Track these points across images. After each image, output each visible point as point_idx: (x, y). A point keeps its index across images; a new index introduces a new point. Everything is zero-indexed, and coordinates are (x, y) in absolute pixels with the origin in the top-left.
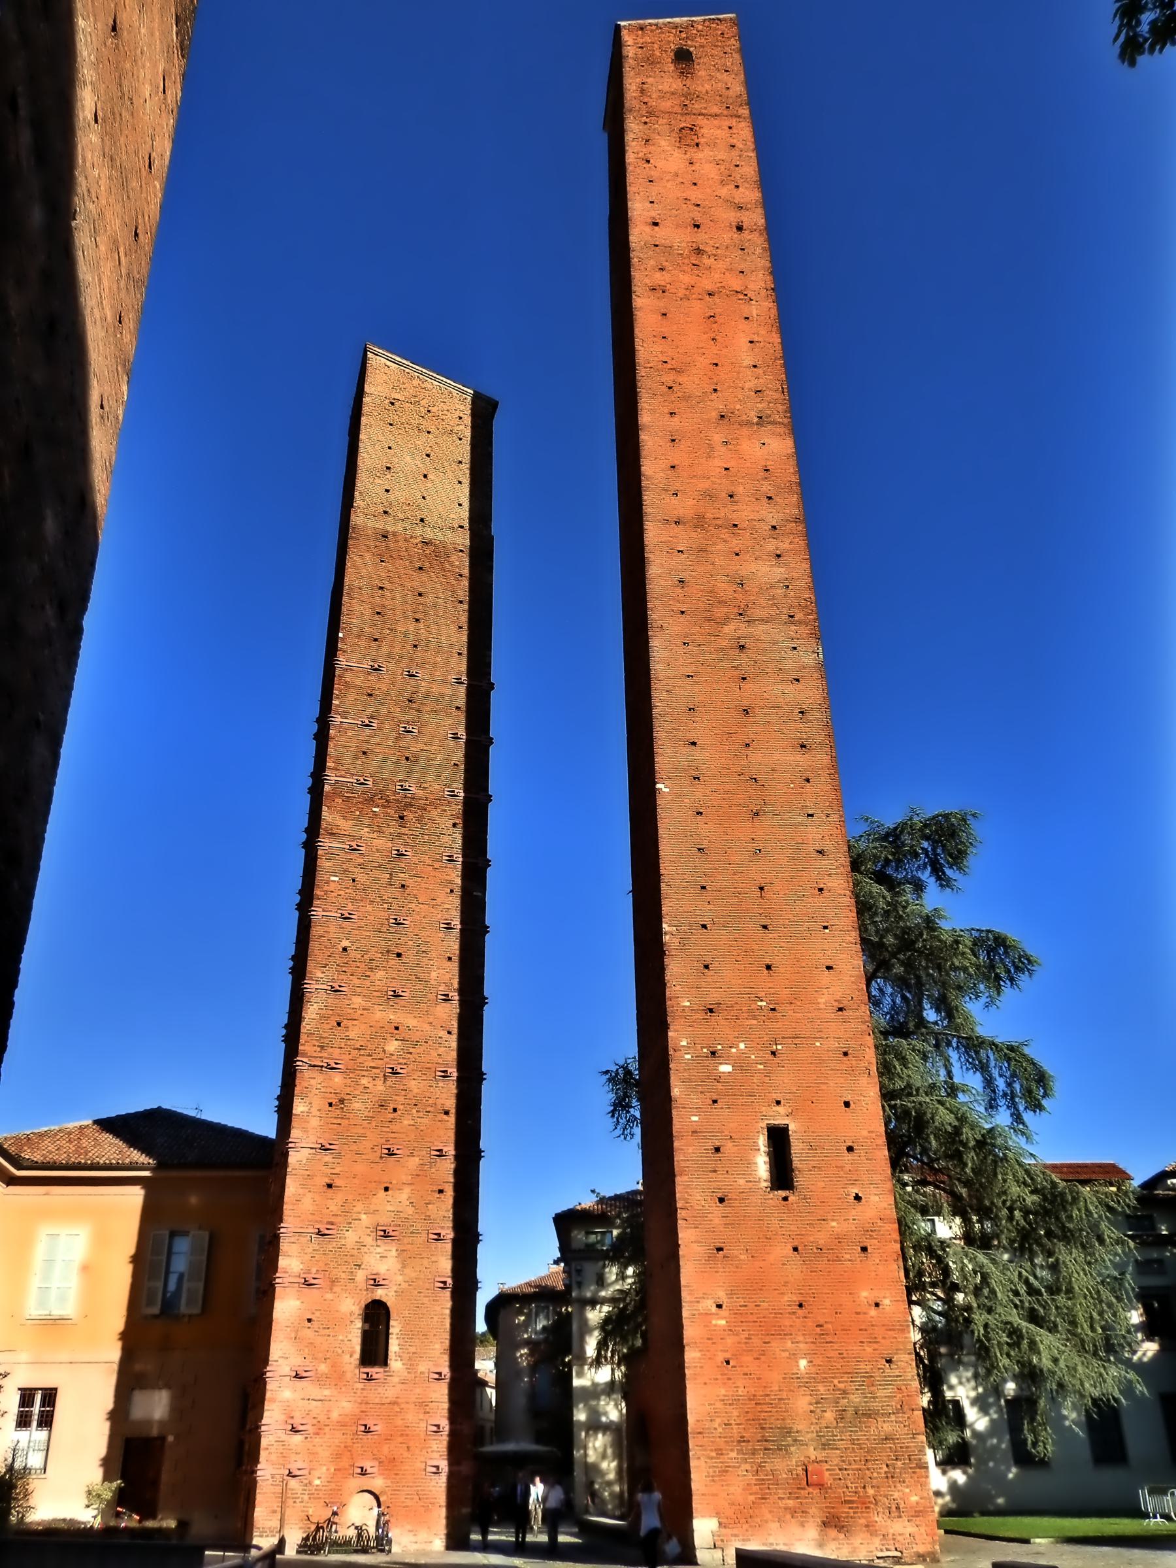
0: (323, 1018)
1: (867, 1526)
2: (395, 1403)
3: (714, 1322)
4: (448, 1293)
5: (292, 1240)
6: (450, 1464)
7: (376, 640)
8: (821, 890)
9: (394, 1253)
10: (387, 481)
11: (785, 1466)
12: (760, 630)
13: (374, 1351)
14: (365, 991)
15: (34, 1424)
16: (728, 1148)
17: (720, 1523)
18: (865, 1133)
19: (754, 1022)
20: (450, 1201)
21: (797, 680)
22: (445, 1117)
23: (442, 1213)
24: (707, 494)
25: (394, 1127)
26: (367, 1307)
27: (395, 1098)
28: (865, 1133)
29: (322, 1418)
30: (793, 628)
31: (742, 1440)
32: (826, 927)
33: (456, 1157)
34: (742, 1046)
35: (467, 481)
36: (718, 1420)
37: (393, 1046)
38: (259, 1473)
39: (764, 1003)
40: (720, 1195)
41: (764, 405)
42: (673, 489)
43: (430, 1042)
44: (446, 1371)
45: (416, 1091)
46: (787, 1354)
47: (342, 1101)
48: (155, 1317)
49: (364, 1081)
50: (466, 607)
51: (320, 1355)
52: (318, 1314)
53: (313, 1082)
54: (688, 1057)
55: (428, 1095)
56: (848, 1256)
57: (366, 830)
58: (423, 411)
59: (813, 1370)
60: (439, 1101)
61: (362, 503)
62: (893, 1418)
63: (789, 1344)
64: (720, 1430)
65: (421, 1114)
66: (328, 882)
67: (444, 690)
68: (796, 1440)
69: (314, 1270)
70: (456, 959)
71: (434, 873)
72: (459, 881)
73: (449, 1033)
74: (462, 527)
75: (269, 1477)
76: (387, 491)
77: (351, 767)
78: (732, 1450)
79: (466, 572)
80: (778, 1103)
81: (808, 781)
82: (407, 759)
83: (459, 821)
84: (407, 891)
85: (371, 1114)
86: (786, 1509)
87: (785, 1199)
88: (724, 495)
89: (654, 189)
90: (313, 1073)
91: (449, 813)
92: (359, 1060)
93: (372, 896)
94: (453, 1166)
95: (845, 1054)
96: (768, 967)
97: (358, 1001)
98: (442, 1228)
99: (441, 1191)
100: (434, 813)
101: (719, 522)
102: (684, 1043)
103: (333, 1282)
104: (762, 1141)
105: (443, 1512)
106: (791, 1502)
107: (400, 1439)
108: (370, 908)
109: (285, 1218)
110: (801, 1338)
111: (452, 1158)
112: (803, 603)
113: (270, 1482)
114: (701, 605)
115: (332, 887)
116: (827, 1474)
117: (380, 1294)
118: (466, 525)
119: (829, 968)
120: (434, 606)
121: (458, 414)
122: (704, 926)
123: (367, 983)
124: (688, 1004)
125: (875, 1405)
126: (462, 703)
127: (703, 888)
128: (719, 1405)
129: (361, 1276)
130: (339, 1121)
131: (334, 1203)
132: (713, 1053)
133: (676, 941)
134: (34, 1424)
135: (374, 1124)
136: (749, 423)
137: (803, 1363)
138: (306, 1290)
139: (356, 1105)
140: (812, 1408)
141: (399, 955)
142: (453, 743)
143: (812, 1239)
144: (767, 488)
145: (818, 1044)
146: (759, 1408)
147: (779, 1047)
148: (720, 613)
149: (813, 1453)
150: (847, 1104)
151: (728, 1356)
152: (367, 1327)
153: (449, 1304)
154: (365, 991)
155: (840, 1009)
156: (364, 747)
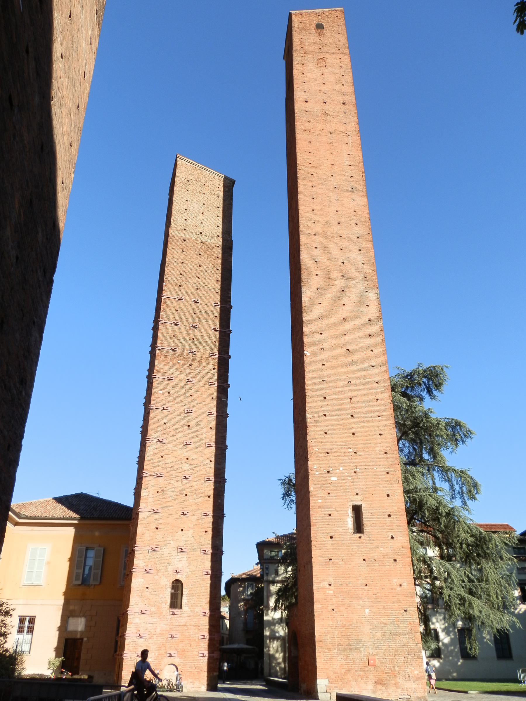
0: (155, 454)
1: (395, 684)
2: (185, 625)
3: (327, 592)
4: (209, 577)
5: (140, 552)
6: (209, 653)
7: (180, 286)
8: (377, 399)
9: (185, 559)
10: (185, 215)
11: (358, 657)
12: (351, 283)
13: (176, 602)
14: (174, 442)
15: (25, 631)
16: (334, 514)
17: (329, 682)
18: (396, 509)
19: (347, 458)
20: (210, 536)
21: (368, 306)
22: (209, 498)
23: (206, 542)
24: (328, 222)
25: (185, 503)
26: (173, 582)
27: (186, 490)
28: (396, 509)
29: (152, 631)
30: (366, 282)
31: (340, 645)
32: (379, 416)
33: (213, 516)
34: (341, 469)
35: (221, 216)
36: (329, 636)
37: (186, 467)
38: (124, 655)
39: (351, 450)
40: (331, 535)
41: (354, 183)
42: (313, 220)
43: (202, 465)
44: (208, 612)
45: (195, 487)
46: (360, 607)
47: (163, 491)
48: (79, 585)
49: (173, 482)
50: (220, 271)
51: (152, 603)
52: (151, 585)
53: (150, 482)
54: (317, 473)
55: (201, 488)
56: (388, 564)
57: (175, 370)
58: (202, 184)
59: (372, 614)
60: (206, 492)
61: (175, 226)
62: (407, 636)
63: (361, 602)
64: (330, 640)
65: (198, 497)
67: (210, 308)
68: (363, 645)
69: (150, 566)
70: (214, 428)
71: (204, 390)
72: (215, 394)
73: (211, 461)
74: (218, 236)
75: (129, 657)
76: (186, 220)
77: (168, 342)
78: (335, 649)
79: (220, 256)
80: (357, 494)
81: (372, 351)
82: (193, 339)
83: (216, 367)
84: (193, 398)
85: (175, 497)
86: (359, 676)
87: (360, 537)
88: (336, 223)
89: (306, 86)
90: (151, 478)
91: (211, 363)
92: (170, 473)
93: (177, 400)
94: (212, 520)
95: (388, 473)
96: (354, 434)
97: (170, 446)
98: (207, 548)
99: (206, 532)
100: (205, 363)
101: (333, 235)
102: (315, 467)
103: (158, 571)
104: (350, 512)
105: (206, 674)
106: (361, 672)
107: (187, 641)
108: (176, 405)
109: (137, 542)
110: (366, 600)
111: (211, 517)
112: (371, 271)
113: (129, 659)
114: (325, 271)
115: (159, 396)
116: (377, 661)
117: (179, 577)
118: (221, 235)
119: (381, 434)
120: (206, 271)
121: (217, 186)
122: (325, 415)
123: (175, 438)
124: (317, 450)
125: (399, 630)
126: (218, 315)
127: (325, 398)
128: (329, 629)
129: (170, 569)
130: (161, 500)
131: (159, 535)
132: (328, 472)
133: (312, 421)
134: (25, 631)
135: (177, 501)
136: (347, 191)
137: (367, 611)
138: (146, 574)
139: (169, 493)
140: (371, 631)
141: (189, 426)
142: (214, 332)
143: (371, 555)
144: (355, 220)
145: (375, 468)
146: (347, 630)
147: (358, 470)
148: (333, 275)
149: (371, 651)
150: (388, 496)
151: (333, 607)
152: (173, 591)
153: (209, 582)
154: (174, 442)
155: (386, 453)
156: (174, 334)
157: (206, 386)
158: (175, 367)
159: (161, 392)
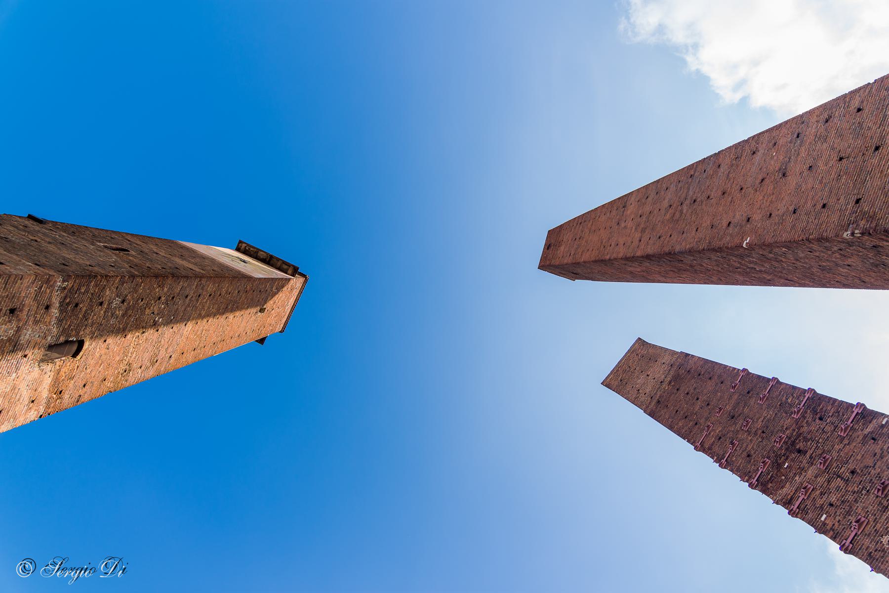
57: (797, 478)
66: (824, 524)
67: (736, 397)
71: (852, 447)
93: (850, 498)
100: (805, 429)
108: (860, 505)
120: (695, 389)
122: (858, 201)
127: (824, 206)
156: (745, 454)
157: (846, 441)
158: (791, 475)
159: (824, 516)
